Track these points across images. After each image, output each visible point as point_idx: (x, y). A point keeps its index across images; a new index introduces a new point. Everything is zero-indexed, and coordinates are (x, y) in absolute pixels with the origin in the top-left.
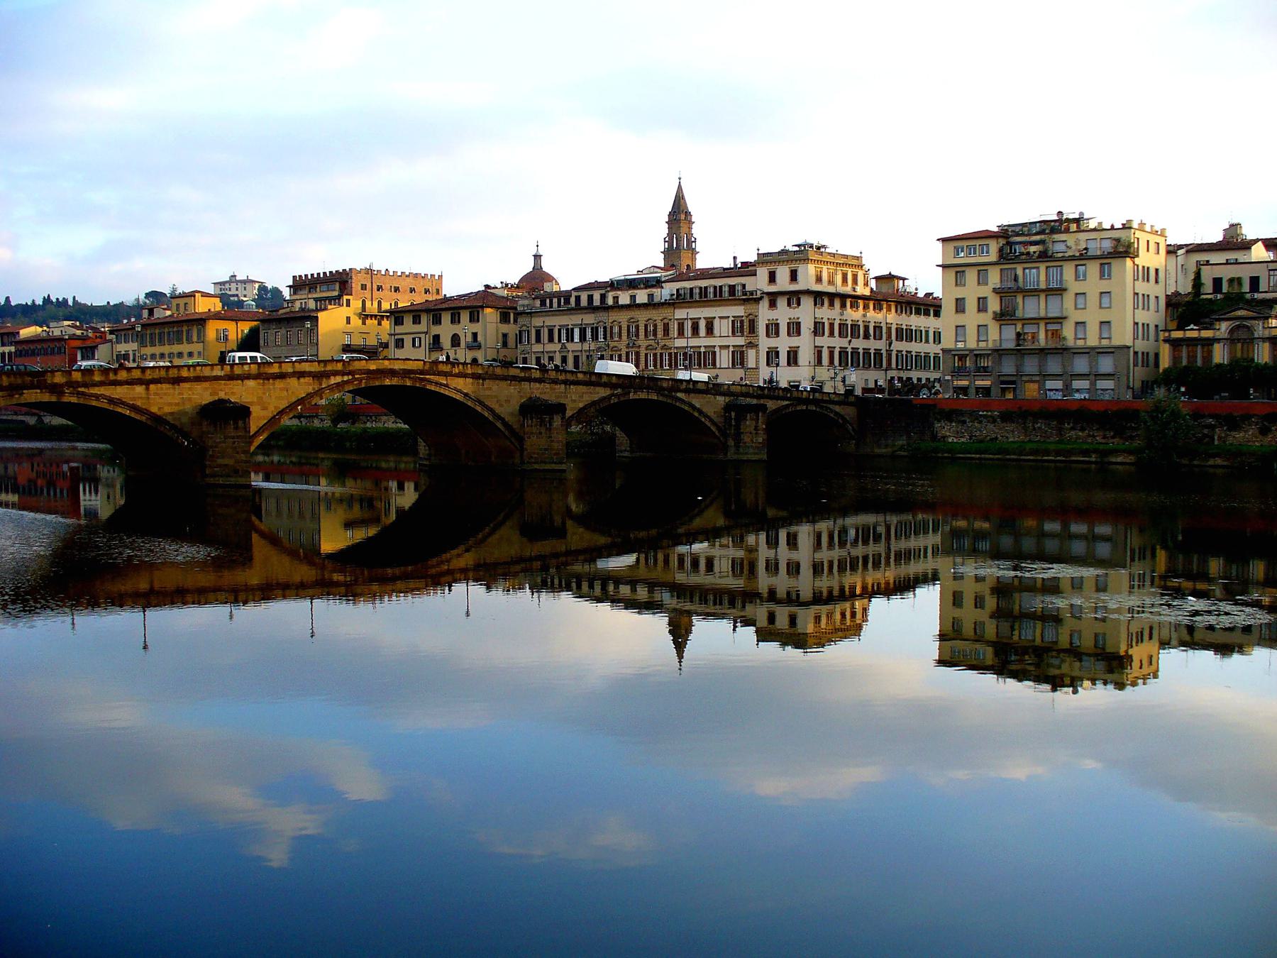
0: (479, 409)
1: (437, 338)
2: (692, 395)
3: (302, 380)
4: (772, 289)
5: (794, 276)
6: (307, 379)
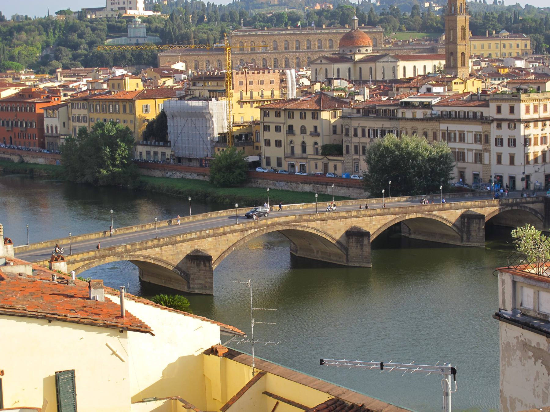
0: (324, 236)
1: (291, 127)
2: (442, 212)
3: (234, 234)
4: (499, 116)
5: (512, 110)
6: (237, 234)
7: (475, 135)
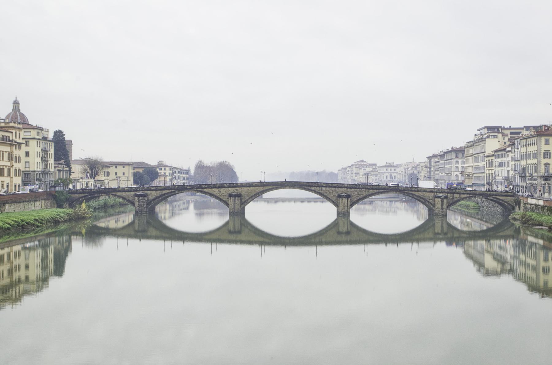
7: (8, 154)
